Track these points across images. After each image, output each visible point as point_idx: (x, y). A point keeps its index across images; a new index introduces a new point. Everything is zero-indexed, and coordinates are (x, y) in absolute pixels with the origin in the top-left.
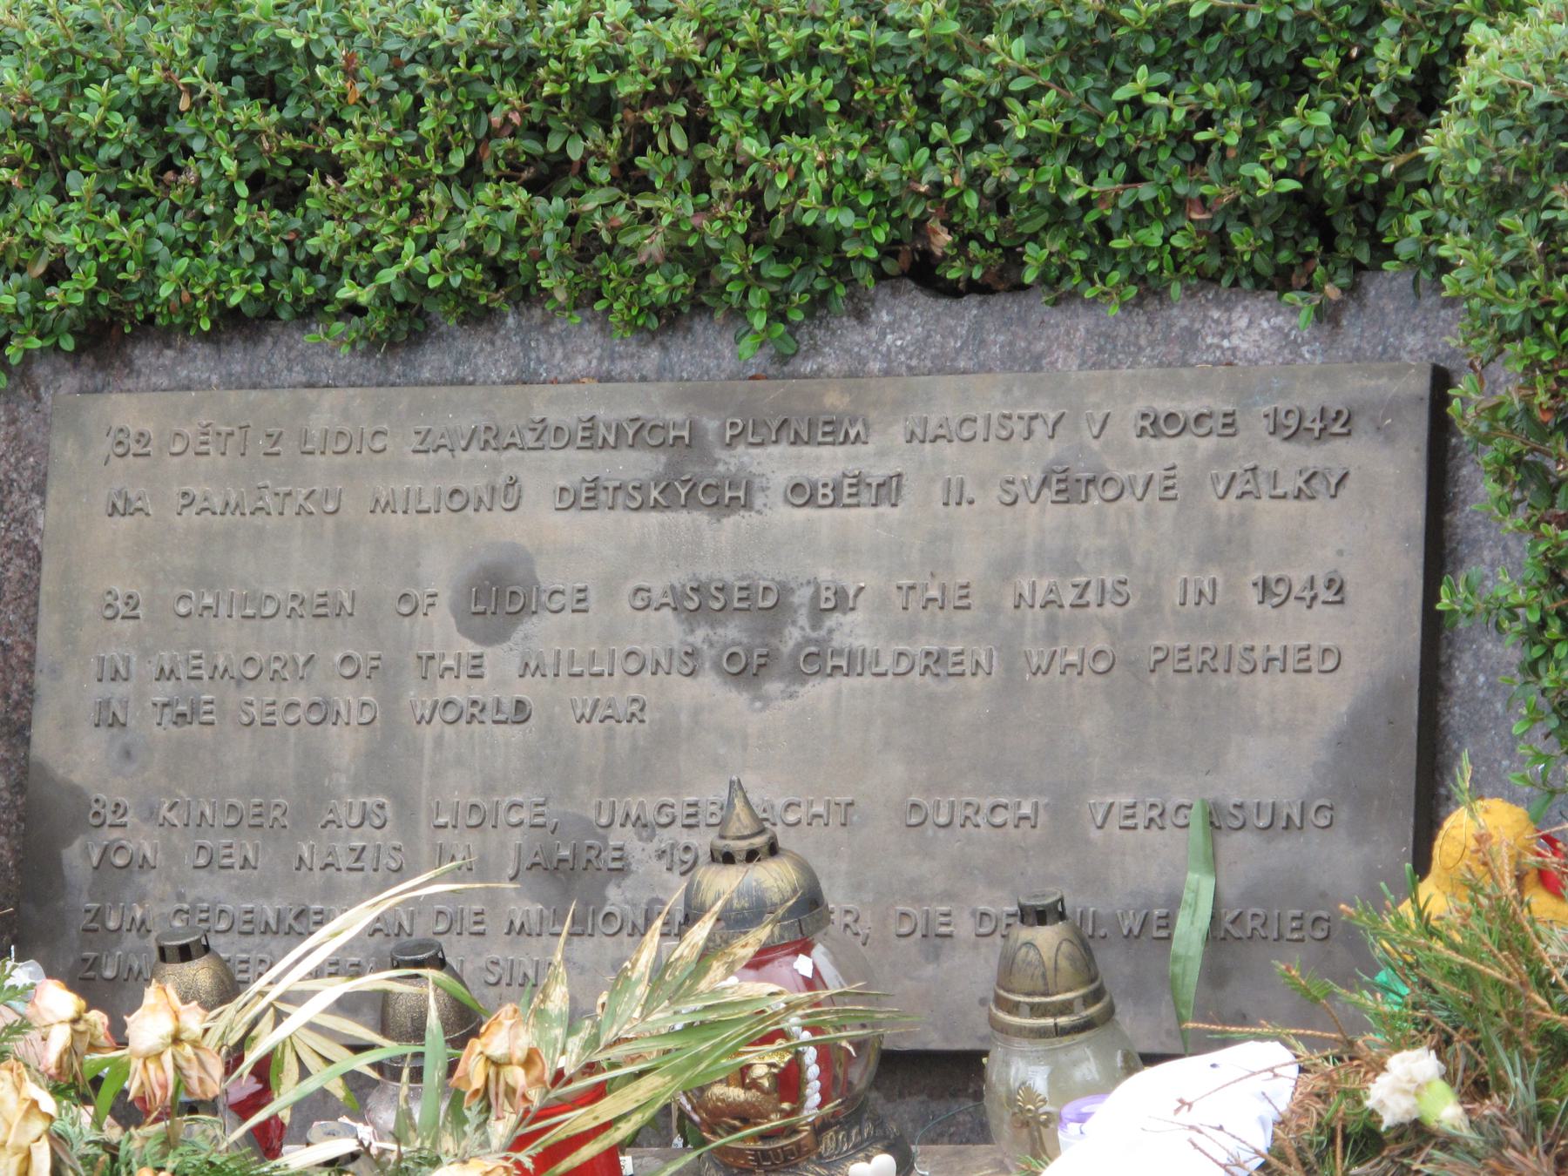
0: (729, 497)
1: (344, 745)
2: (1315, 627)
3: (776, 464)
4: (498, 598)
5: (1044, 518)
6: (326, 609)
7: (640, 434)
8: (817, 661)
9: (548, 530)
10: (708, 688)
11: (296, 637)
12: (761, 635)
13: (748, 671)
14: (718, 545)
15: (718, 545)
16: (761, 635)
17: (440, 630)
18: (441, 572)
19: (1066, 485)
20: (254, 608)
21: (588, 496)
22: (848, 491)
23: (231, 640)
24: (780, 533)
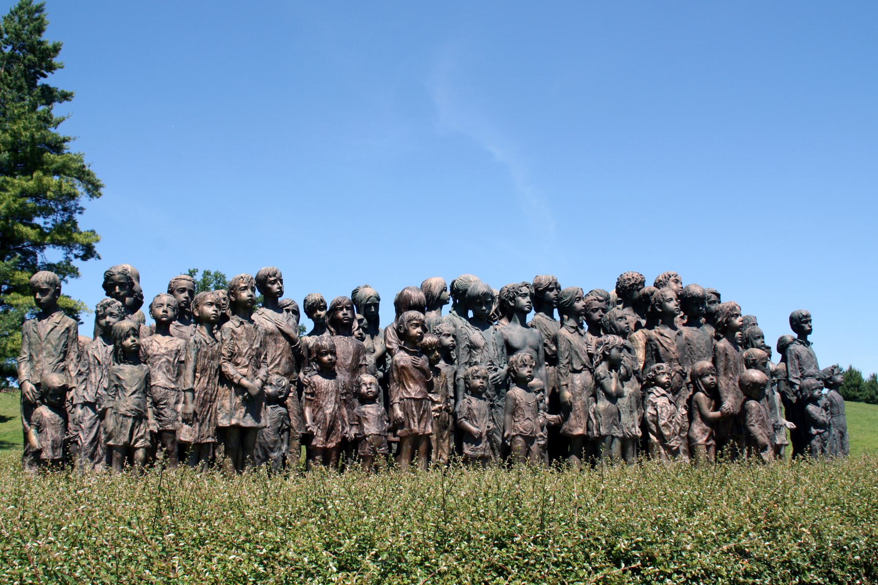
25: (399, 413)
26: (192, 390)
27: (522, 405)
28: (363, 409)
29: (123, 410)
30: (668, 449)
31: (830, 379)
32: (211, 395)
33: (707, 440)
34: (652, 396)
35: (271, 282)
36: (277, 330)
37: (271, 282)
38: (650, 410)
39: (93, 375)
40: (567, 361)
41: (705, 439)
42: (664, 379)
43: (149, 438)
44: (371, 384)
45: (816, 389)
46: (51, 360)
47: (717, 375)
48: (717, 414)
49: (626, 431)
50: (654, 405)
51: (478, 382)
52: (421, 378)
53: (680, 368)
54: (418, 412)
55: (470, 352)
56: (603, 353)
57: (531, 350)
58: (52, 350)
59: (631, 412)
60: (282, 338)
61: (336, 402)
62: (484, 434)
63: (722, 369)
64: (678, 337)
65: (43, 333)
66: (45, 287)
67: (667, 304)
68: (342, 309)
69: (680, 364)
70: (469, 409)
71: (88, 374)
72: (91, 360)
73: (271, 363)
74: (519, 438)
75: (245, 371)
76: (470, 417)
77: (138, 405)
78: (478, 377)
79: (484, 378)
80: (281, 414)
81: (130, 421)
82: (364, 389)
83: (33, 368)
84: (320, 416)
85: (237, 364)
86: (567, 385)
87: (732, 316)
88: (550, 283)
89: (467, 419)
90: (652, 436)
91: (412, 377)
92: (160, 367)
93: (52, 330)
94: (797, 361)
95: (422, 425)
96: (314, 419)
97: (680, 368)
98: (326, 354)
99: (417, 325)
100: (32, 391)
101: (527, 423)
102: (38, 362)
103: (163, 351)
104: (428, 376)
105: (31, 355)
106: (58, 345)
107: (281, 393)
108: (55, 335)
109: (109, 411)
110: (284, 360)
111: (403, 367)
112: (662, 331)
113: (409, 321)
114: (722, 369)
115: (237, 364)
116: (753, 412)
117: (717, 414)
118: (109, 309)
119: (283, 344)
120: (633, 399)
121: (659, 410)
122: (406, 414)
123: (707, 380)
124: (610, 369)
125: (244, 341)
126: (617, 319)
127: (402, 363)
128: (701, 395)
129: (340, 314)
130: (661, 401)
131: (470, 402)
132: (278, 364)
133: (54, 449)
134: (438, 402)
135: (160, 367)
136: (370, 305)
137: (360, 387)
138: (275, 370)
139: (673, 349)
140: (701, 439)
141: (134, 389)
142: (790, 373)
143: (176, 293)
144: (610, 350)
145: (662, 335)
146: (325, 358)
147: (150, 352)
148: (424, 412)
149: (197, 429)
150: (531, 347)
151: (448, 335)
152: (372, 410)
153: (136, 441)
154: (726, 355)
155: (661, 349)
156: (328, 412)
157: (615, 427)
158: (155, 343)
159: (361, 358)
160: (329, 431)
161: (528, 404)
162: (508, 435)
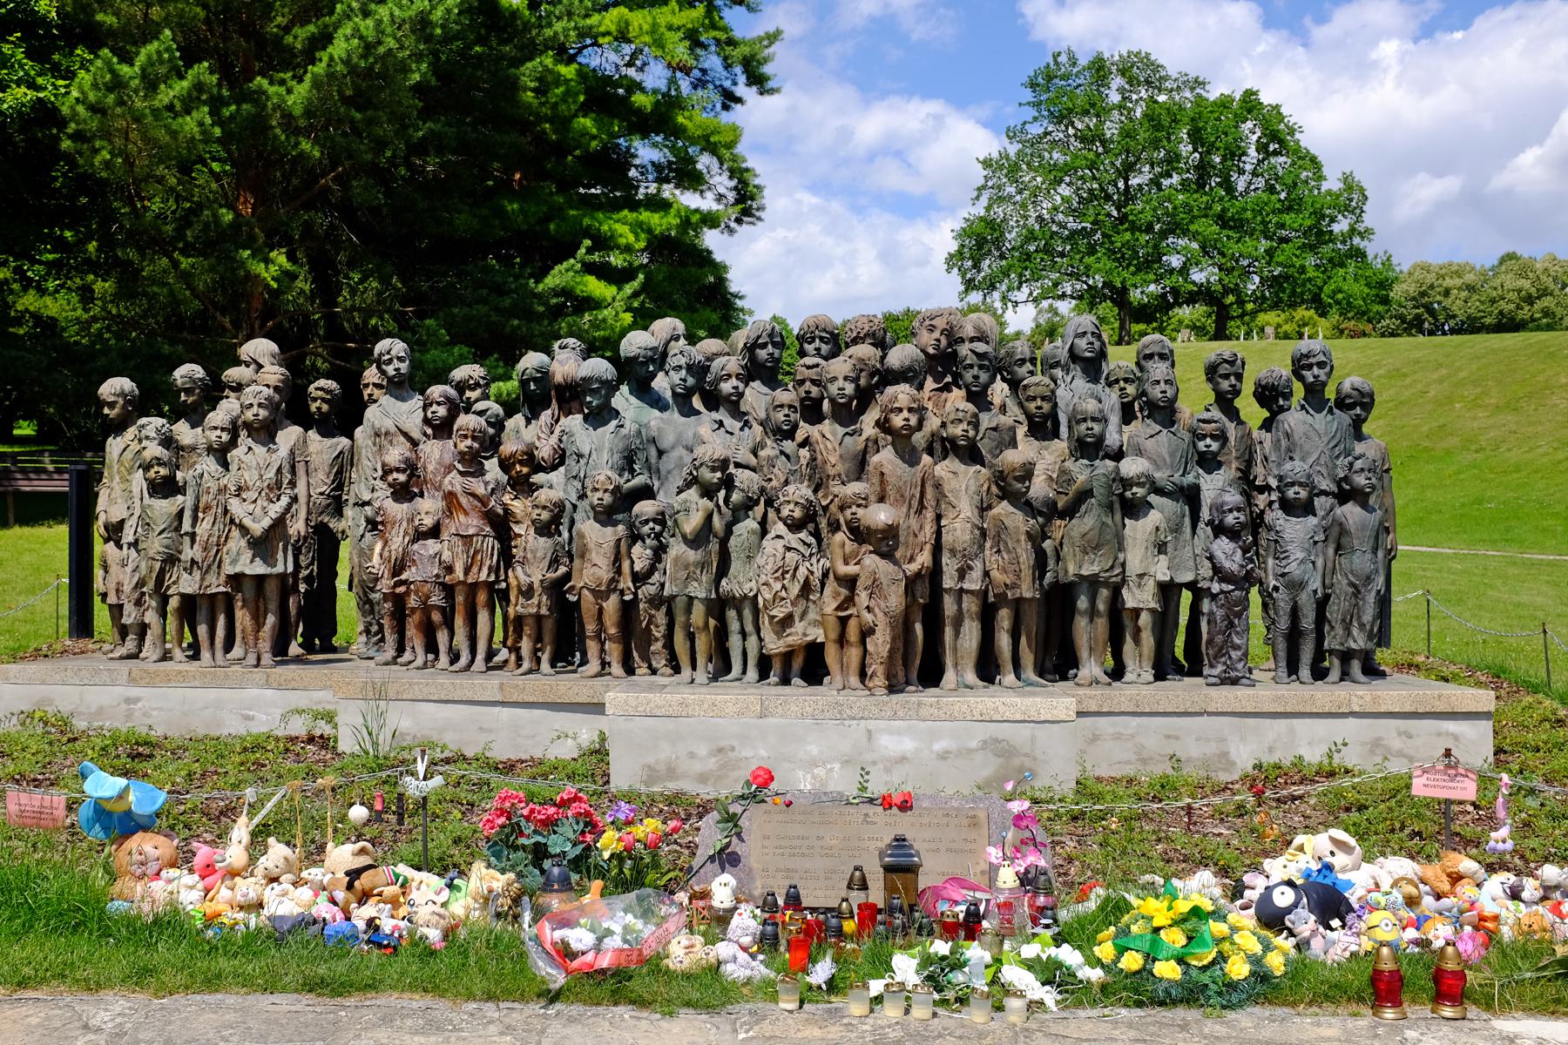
27: (591, 545)
36: (393, 429)
41: (834, 605)
45: (1231, 511)
61: (406, 533)
64: (847, 438)
74: (585, 592)
79: (544, 508)
81: (158, 565)
84: (386, 554)
87: (892, 411)
104: (485, 504)
139: (833, 460)
148: (476, 552)
153: (169, 587)
154: (882, 474)
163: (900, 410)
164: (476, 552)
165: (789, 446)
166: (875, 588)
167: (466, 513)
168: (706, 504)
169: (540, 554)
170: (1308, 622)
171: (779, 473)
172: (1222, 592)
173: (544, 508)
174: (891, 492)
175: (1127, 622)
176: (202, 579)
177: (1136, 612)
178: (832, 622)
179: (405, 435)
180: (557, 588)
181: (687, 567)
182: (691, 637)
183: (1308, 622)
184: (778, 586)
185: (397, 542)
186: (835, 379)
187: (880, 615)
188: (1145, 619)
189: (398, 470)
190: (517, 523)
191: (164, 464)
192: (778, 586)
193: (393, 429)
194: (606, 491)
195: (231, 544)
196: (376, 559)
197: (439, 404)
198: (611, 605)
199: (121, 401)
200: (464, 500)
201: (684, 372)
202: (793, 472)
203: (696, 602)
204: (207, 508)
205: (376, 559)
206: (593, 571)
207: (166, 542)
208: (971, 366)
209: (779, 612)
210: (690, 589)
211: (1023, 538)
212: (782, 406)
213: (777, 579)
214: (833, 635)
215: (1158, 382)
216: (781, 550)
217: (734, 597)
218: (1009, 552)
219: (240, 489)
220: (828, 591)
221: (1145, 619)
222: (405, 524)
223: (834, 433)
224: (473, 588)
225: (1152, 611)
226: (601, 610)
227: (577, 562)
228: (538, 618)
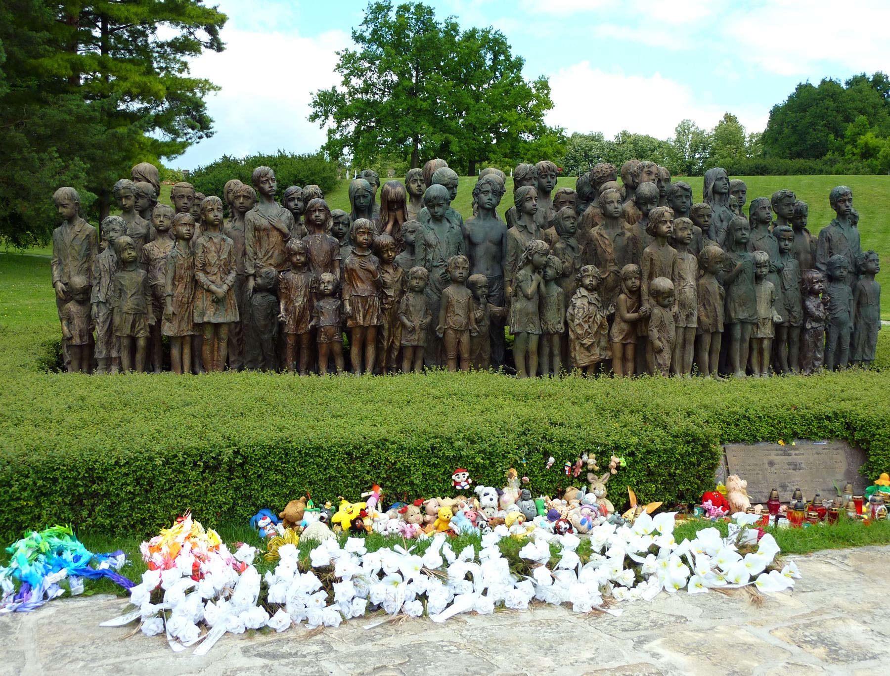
0: (789, 455)
1: (760, 476)
2: (840, 465)
3: (793, 452)
4: (771, 464)
5: (816, 456)
6: (756, 465)
7: (780, 450)
8: (800, 468)
9: (773, 457)
10: (791, 471)
11: (754, 467)
12: (795, 467)
13: (795, 469)
14: (790, 459)
15: (790, 459)
16: (795, 467)
17: (767, 466)
18: (766, 462)
19: (818, 454)
20: (749, 465)
21: (777, 455)
22: (799, 454)
23: (748, 468)
24: (794, 457)
25: (348, 308)
26: (172, 296)
27: (454, 302)
28: (321, 304)
29: (125, 309)
30: (582, 345)
31: (864, 265)
32: (189, 298)
33: (624, 339)
34: (575, 296)
35: (263, 182)
36: (269, 227)
37: (263, 182)
38: (570, 310)
39: (103, 280)
40: (513, 258)
42: (587, 282)
43: (148, 330)
44: (328, 282)
45: (817, 282)
46: (76, 263)
47: (640, 279)
48: (635, 315)
49: (550, 327)
50: (574, 306)
51: (414, 282)
52: (368, 278)
53: (616, 268)
54: (364, 307)
55: (426, 249)
56: (527, 258)
57: (490, 244)
58: (76, 255)
59: (559, 310)
60: (276, 233)
61: (305, 295)
62: (417, 328)
63: (646, 275)
64: (617, 238)
65: (68, 240)
66: (66, 202)
67: (608, 206)
68: (315, 211)
69: (616, 264)
70: (407, 305)
71: (100, 279)
72: (102, 267)
73: (264, 256)
74: (450, 332)
75: (214, 278)
76: (407, 313)
77: (138, 305)
78: (416, 278)
80: (270, 302)
81: (131, 318)
82: (322, 287)
83: (62, 270)
84: (291, 308)
85: (208, 273)
86: (511, 281)
87: (660, 222)
88: (527, 174)
89: (405, 314)
90: (570, 333)
91: (359, 277)
92: (160, 269)
93: (75, 238)
94: (827, 245)
95: (368, 317)
96: (286, 310)
97: (616, 268)
98: (295, 254)
99: (364, 233)
100: (63, 291)
101: (455, 318)
102: (66, 265)
103: (162, 255)
104: (374, 276)
105: (60, 259)
106: (80, 251)
107: (269, 283)
108: (77, 243)
109: (116, 310)
110: (277, 252)
111: (352, 269)
112: (603, 232)
113: (357, 229)
114: (646, 275)
115: (208, 273)
116: (653, 318)
117: (635, 315)
118: (111, 225)
119: (275, 238)
120: (561, 297)
121: (576, 311)
122: (353, 309)
123: (629, 283)
124: (534, 272)
125: (213, 253)
126: (564, 219)
127: (351, 266)
128: (623, 296)
129: (313, 216)
130: (578, 303)
131: (408, 300)
132: (271, 257)
133: (81, 337)
134: (391, 296)
135: (160, 269)
136: (359, 197)
137: (320, 285)
138: (269, 262)
139: (609, 250)
140: (617, 339)
141: (133, 292)
142: (818, 256)
143: (176, 199)
144: (532, 255)
145: (602, 236)
146: (295, 259)
147: (151, 256)
148: (370, 307)
149: (177, 325)
150: (491, 241)
151: (413, 232)
152: (328, 305)
153: (139, 332)
154: (652, 259)
155: (599, 250)
156: (297, 304)
157: (531, 325)
158: (155, 249)
159: (335, 253)
160: (299, 321)
161: (458, 301)
162: (440, 328)
163: (666, 222)
164: (370, 307)
165: (573, 241)
166: (662, 327)
167: (363, 282)
168: (537, 277)
169: (418, 308)
170: (846, 345)
171: (570, 257)
172: (812, 328)
173: (421, 278)
174: (657, 269)
175: (755, 346)
176: (179, 326)
177: (762, 339)
178: (618, 348)
179: (278, 230)
180: (430, 329)
181: (527, 314)
182: (527, 358)
183: (846, 345)
184: (586, 326)
185: (299, 302)
186: (613, 202)
187: (665, 342)
188: (766, 344)
189: (300, 254)
190: (388, 288)
191: (133, 248)
192: (586, 326)
193: (269, 227)
194: (464, 268)
195: (199, 303)
196: (283, 313)
197: (320, 210)
198: (465, 338)
199: (72, 205)
200: (361, 274)
201: (490, 195)
202: (575, 258)
203: (531, 336)
204: (181, 278)
205: (283, 313)
206: (457, 318)
207: (135, 302)
208: (681, 196)
209: (587, 341)
210: (529, 328)
211: (718, 297)
212: (568, 217)
213: (585, 322)
214: (618, 354)
215: (765, 208)
216: (587, 304)
217: (549, 333)
218: (710, 305)
219: (204, 265)
220: (615, 329)
221: (766, 344)
222: (304, 289)
223: (609, 234)
224: (364, 329)
225: (770, 339)
226: (459, 342)
227: (442, 313)
228: (415, 348)
